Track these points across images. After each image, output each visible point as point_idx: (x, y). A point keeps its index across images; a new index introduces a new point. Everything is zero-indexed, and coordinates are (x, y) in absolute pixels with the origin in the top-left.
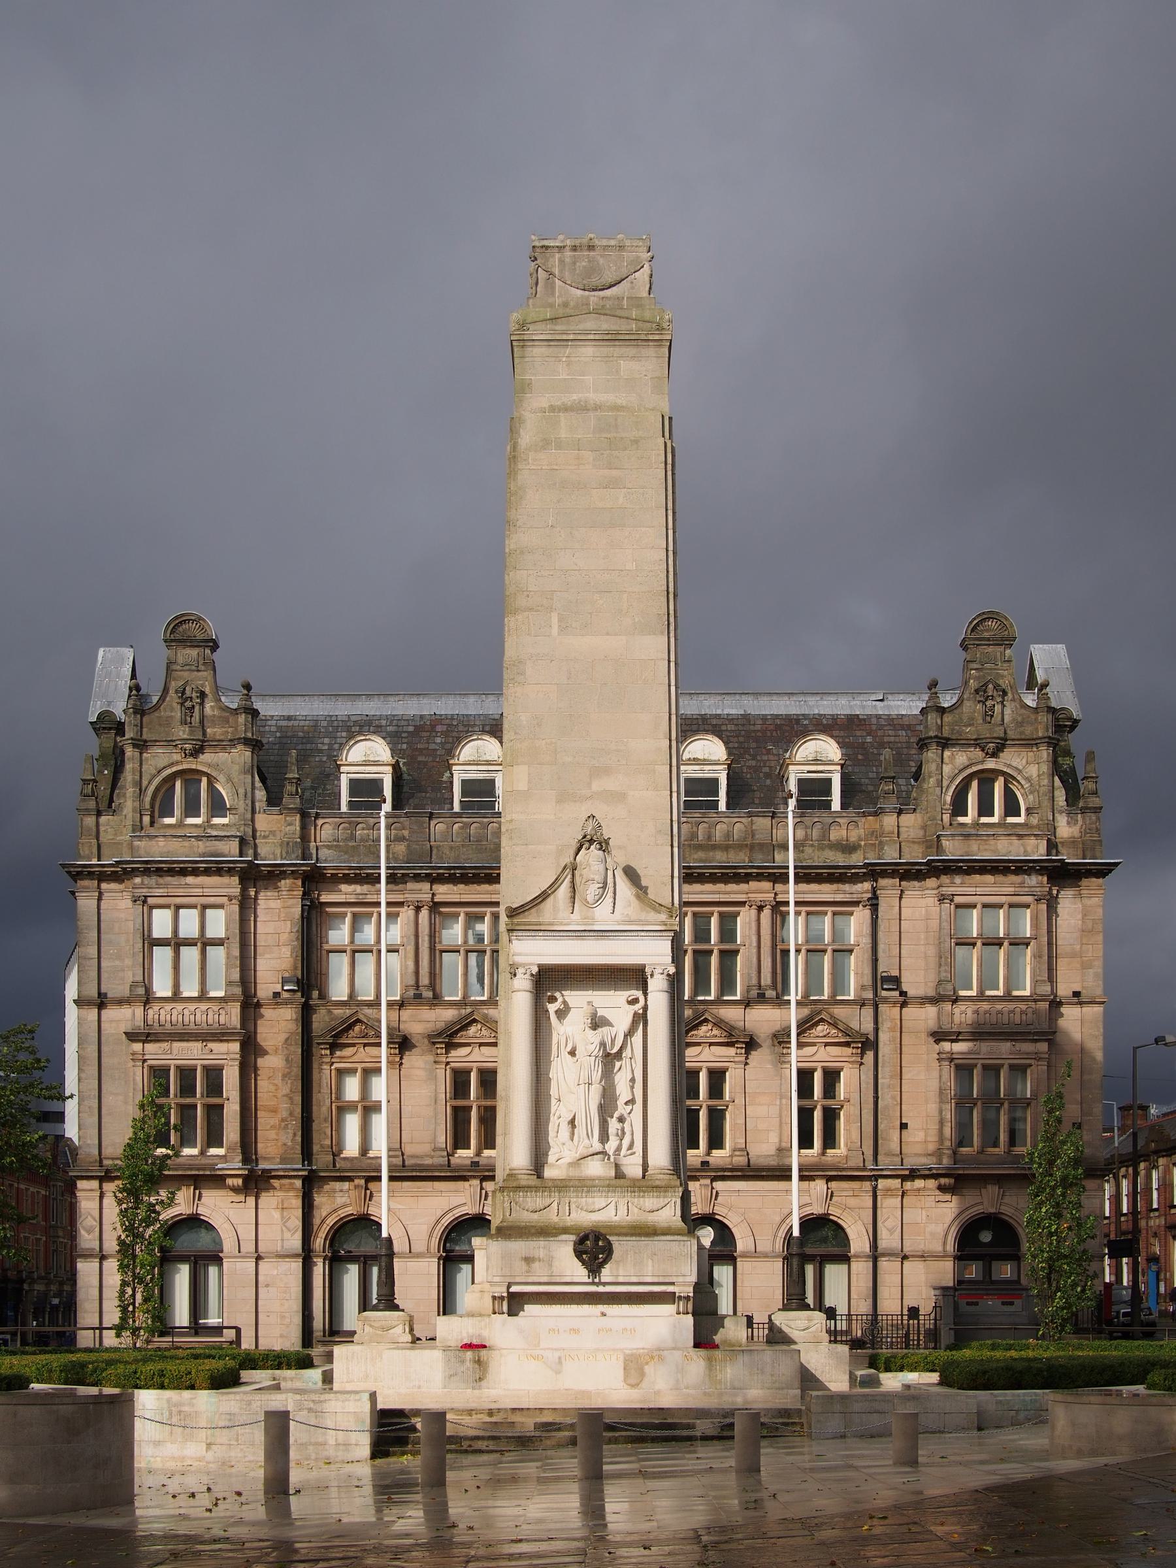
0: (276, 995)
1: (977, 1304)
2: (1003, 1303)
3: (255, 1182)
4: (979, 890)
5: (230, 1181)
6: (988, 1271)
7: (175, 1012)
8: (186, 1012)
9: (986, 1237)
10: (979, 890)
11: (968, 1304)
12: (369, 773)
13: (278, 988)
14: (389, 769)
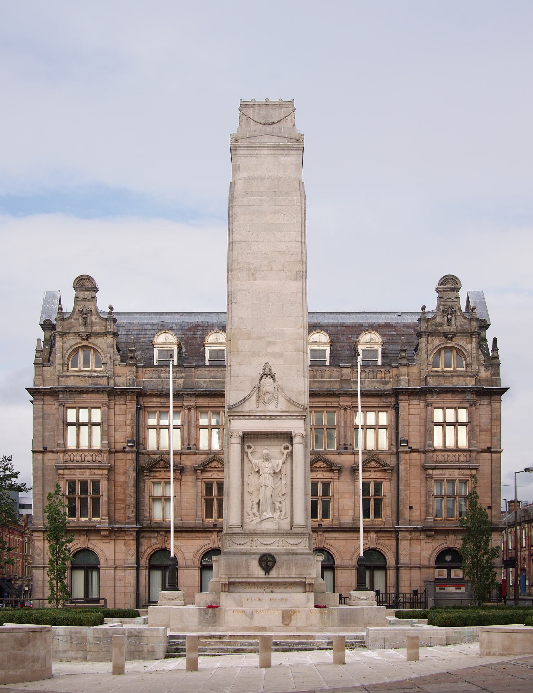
0: (124, 448)
1: (444, 589)
2: (456, 589)
3: (114, 532)
4: (445, 401)
5: (103, 533)
6: (449, 574)
7: (78, 456)
8: (83, 456)
9: (448, 558)
10: (445, 401)
11: (440, 589)
12: (168, 347)
13: (125, 445)
14: (176, 346)
